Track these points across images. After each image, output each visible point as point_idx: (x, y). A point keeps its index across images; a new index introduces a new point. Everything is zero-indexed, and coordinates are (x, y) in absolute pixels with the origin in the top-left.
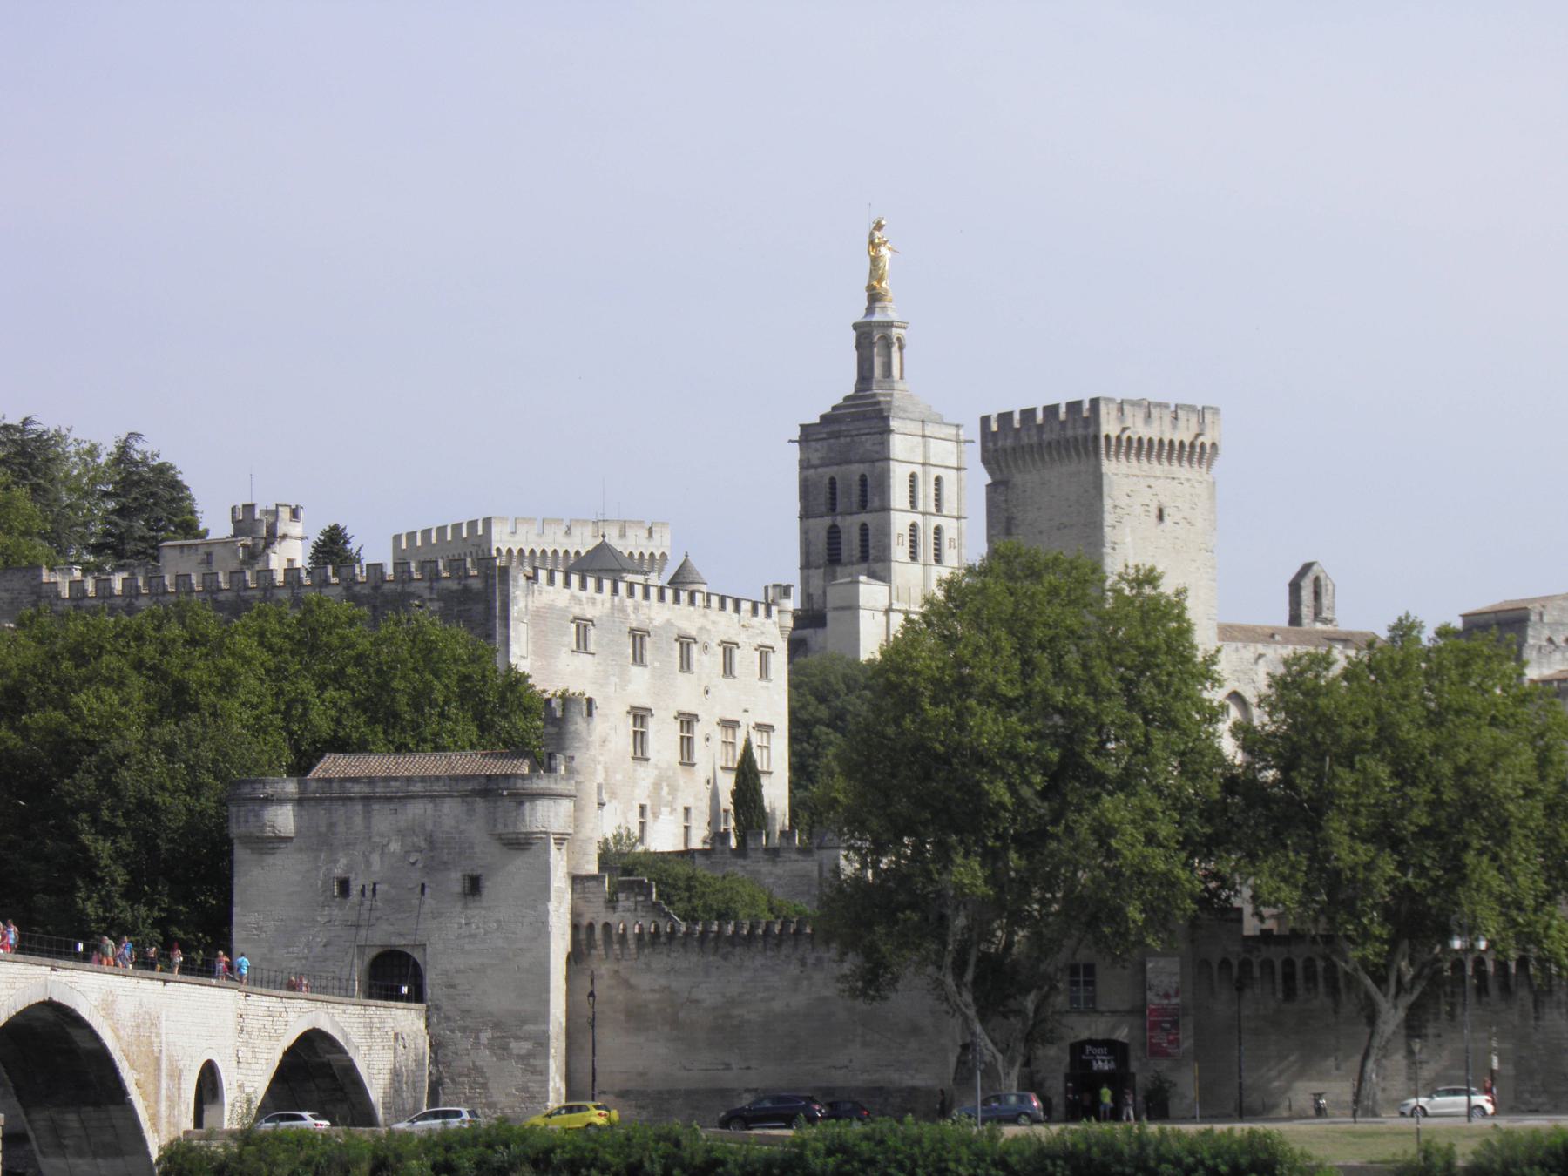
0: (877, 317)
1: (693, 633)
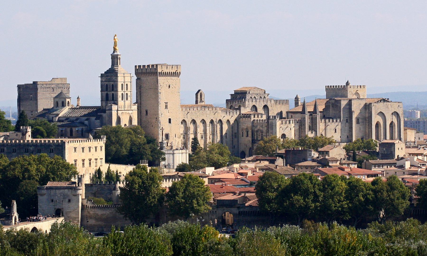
0: (115, 54)
1: (91, 146)
